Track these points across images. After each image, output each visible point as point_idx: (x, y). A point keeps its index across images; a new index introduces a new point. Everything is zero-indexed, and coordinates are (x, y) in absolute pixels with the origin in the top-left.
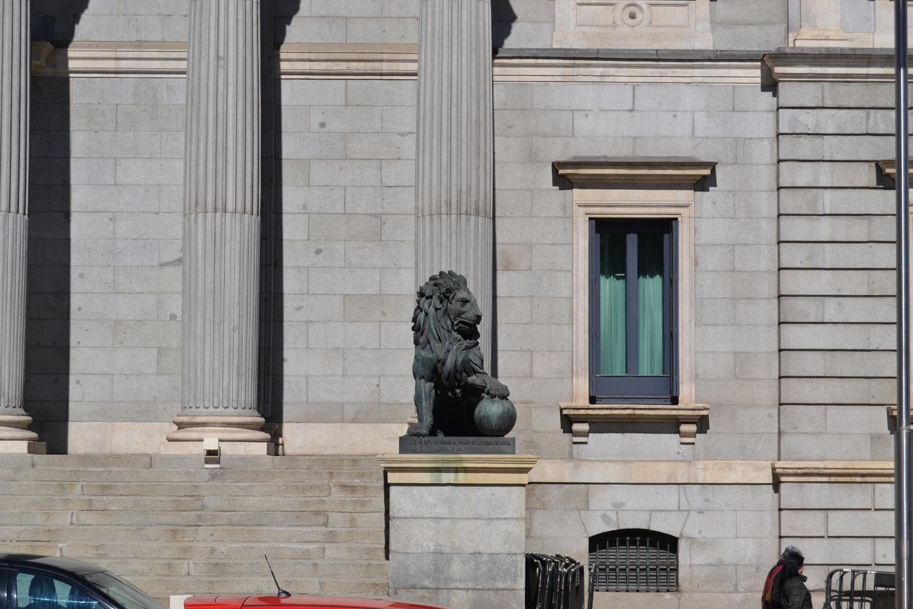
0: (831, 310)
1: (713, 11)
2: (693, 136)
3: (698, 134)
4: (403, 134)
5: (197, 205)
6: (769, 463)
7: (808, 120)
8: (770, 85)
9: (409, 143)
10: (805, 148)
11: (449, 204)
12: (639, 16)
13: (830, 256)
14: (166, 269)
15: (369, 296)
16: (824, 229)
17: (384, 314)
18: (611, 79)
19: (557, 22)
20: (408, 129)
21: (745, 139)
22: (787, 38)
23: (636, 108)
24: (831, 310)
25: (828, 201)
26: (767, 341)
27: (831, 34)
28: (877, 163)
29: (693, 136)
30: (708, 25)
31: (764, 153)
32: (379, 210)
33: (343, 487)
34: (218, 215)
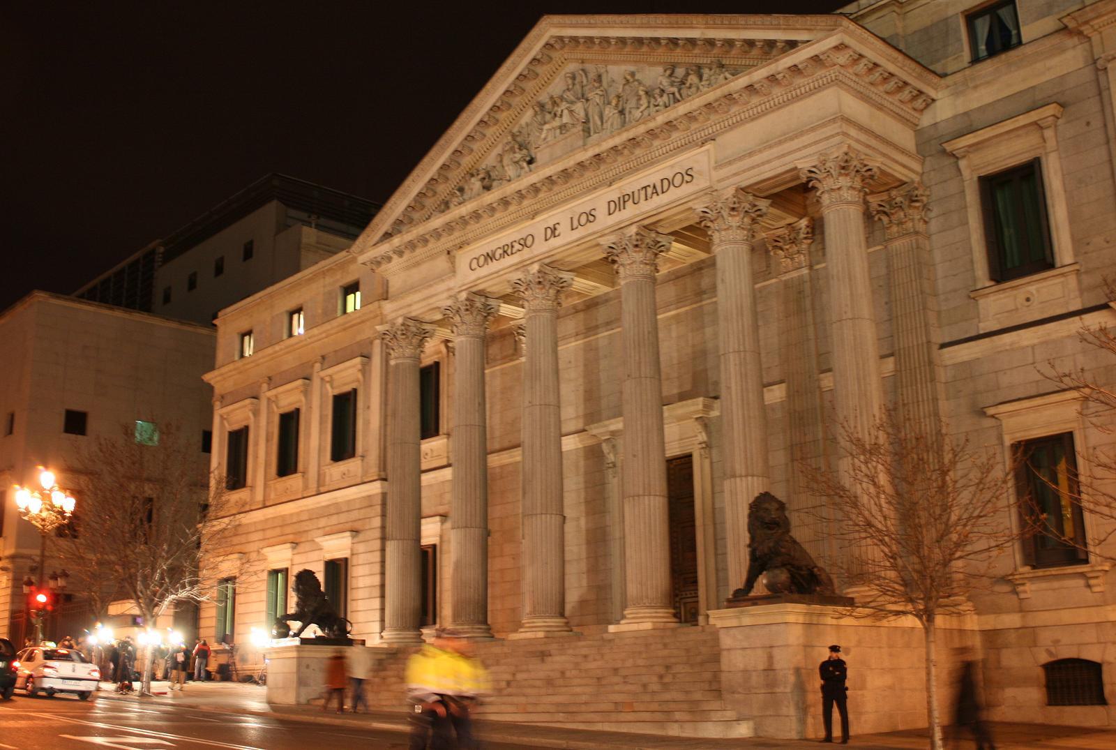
19: (981, 316)
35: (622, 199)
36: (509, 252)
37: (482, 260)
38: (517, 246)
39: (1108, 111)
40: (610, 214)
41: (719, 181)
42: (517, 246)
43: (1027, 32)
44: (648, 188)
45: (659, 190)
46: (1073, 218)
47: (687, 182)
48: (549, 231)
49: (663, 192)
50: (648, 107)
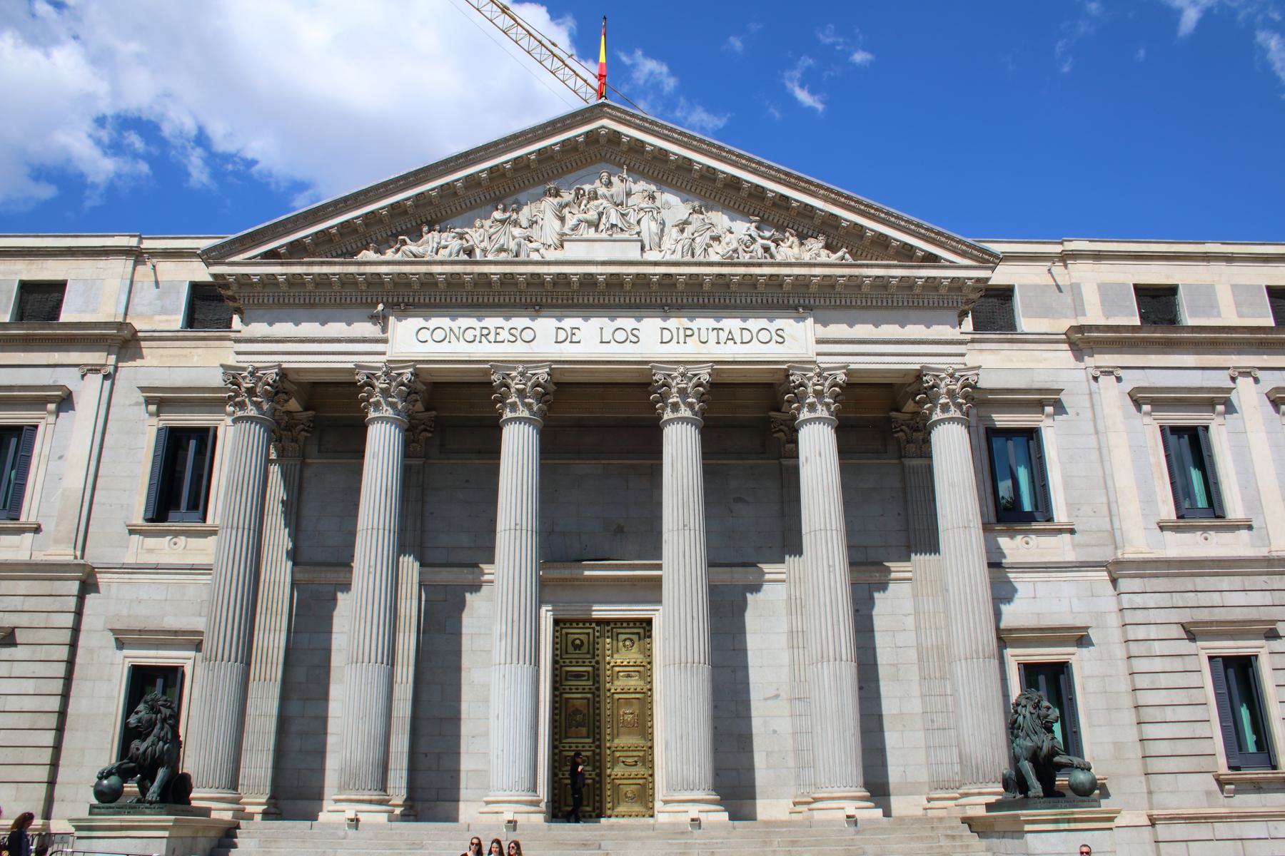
0: (1169, 714)
1: (1072, 539)
2: (1072, 611)
3: (1074, 611)
4: (905, 615)
5: (822, 657)
6: (1144, 812)
7: (1139, 600)
8: (1114, 581)
9: (910, 622)
10: (1139, 616)
11: (977, 652)
12: (1031, 543)
13: (1163, 680)
14: (769, 701)
15: (894, 715)
16: (1158, 664)
17: (904, 726)
18: (1020, 580)
20: (909, 612)
21: (1101, 613)
22: (1115, 554)
23: (1038, 596)
24: (1169, 714)
25: (1158, 648)
26: (1131, 734)
27: (1143, 550)
28: (1182, 625)
29: (1072, 611)
30: (1071, 547)
31: (1114, 620)
32: (896, 662)
33: (947, 836)
34: (837, 662)
35: (681, 331)
36: (491, 337)
37: (439, 335)
38: (504, 335)
39: (1097, 408)
40: (662, 342)
41: (818, 354)
42: (504, 335)
43: (1025, 323)
44: (720, 331)
45: (738, 341)
46: (1067, 485)
47: (777, 342)
48: (562, 335)
49: (742, 343)
50: (735, 251)
